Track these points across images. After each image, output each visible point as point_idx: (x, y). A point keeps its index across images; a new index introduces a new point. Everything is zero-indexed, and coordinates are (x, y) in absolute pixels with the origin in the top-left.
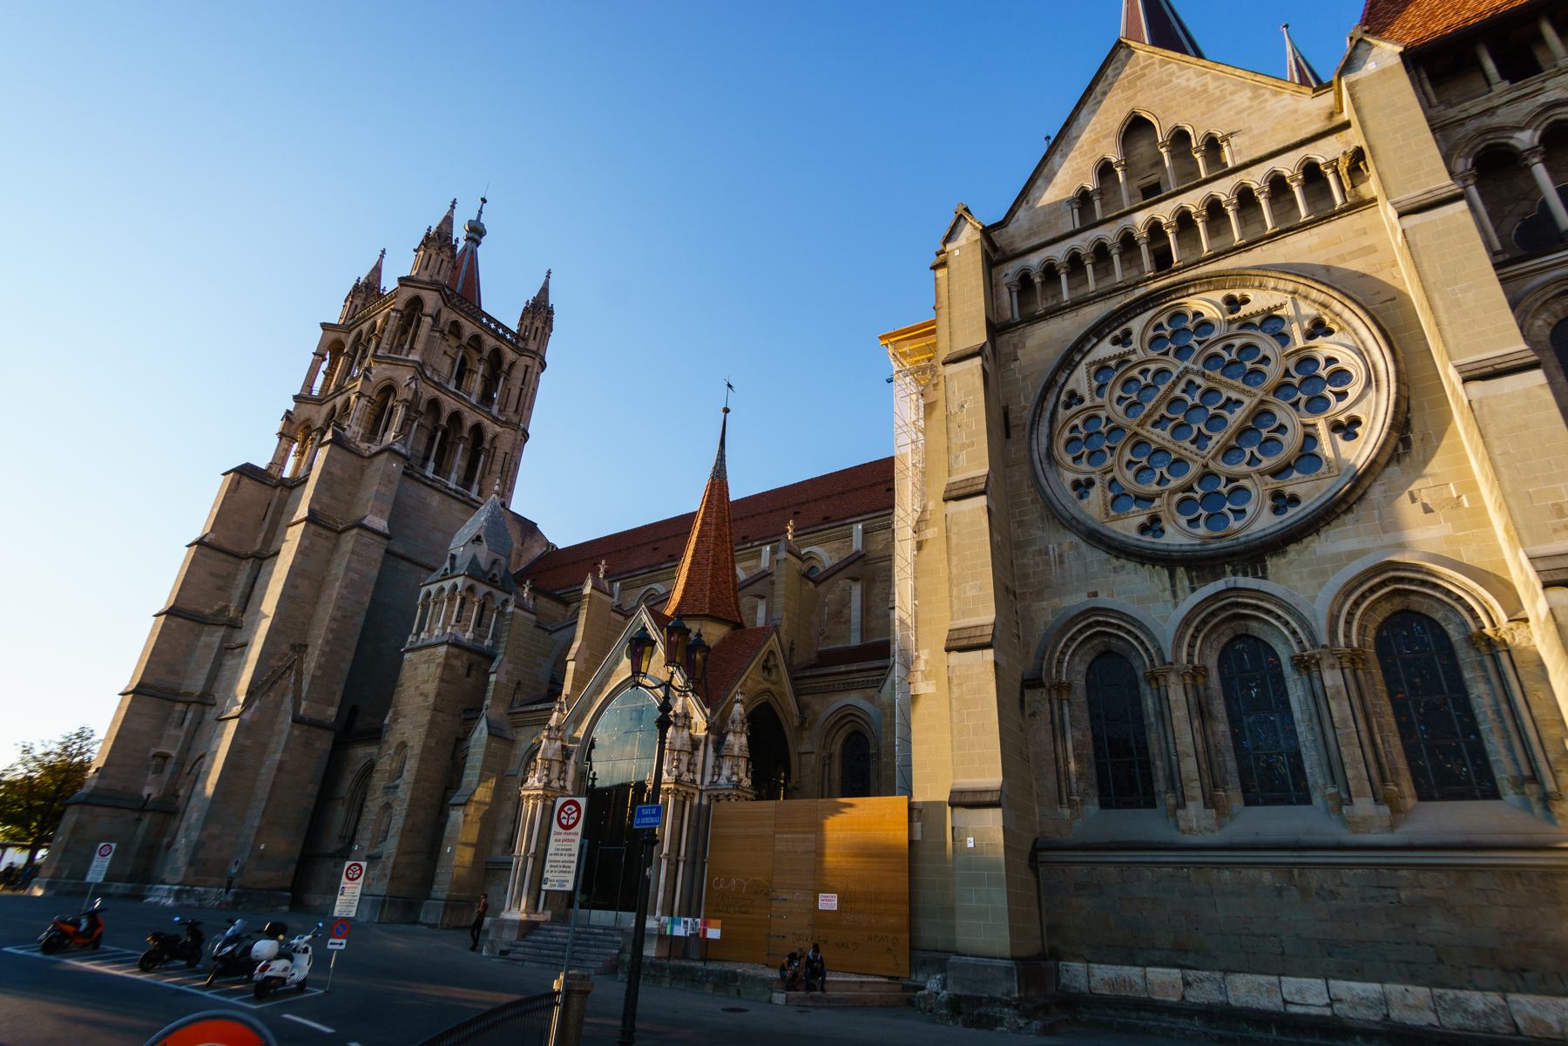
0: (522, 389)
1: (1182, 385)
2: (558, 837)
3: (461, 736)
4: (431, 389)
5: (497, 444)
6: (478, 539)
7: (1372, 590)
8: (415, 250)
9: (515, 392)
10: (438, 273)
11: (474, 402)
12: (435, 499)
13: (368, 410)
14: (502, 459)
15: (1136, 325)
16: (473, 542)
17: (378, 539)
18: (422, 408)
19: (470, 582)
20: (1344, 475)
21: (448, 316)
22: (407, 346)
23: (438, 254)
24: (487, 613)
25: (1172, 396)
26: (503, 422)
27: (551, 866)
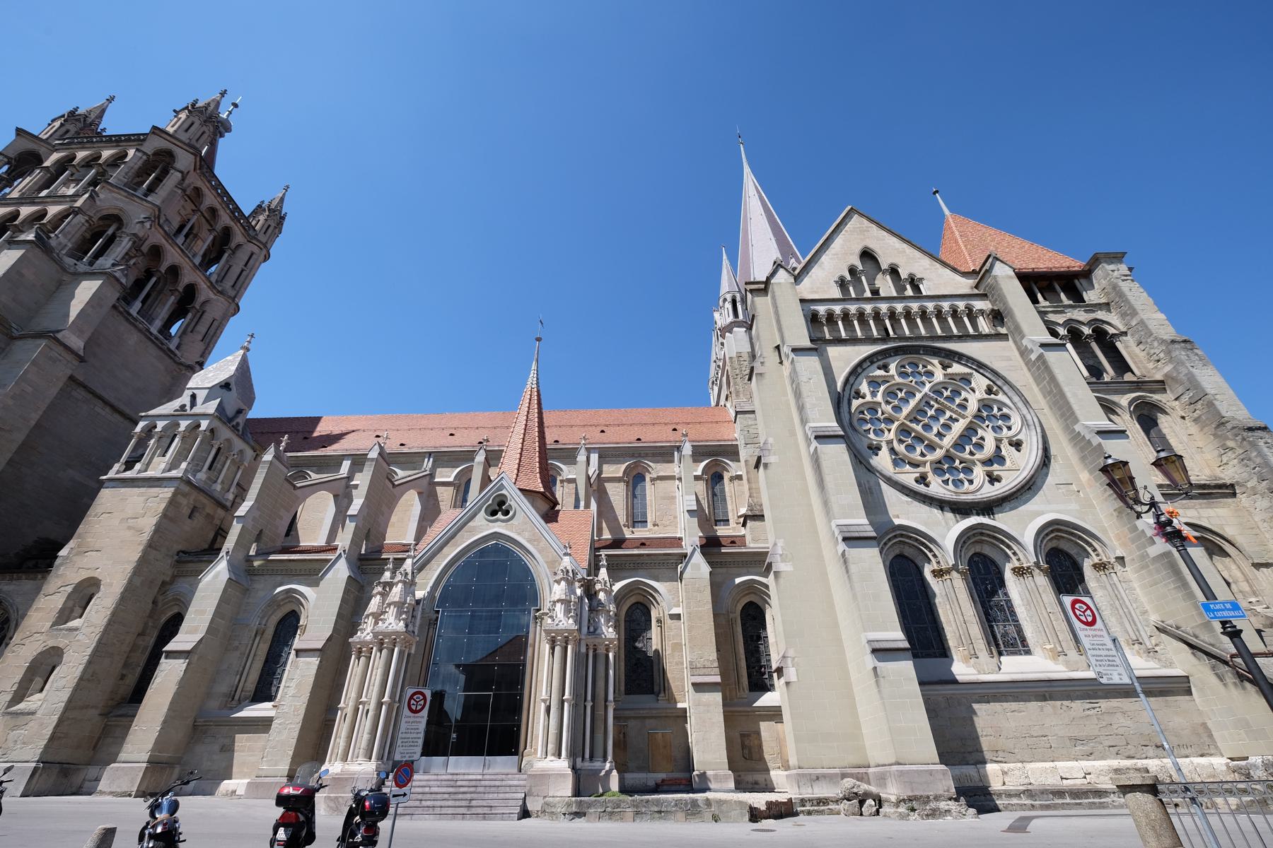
0: (242, 271)
1: (923, 403)
2: (1086, 633)
3: (168, 579)
4: (159, 236)
5: (207, 308)
7: (1047, 535)
8: (175, 111)
9: (235, 270)
10: (197, 140)
11: (197, 264)
12: (133, 338)
13: (84, 228)
14: (209, 324)
16: (221, 387)
17: (69, 357)
18: (145, 248)
19: (217, 424)
20: (1023, 470)
21: (195, 180)
24: (221, 458)
25: (919, 408)
26: (219, 292)
27: (1097, 660)
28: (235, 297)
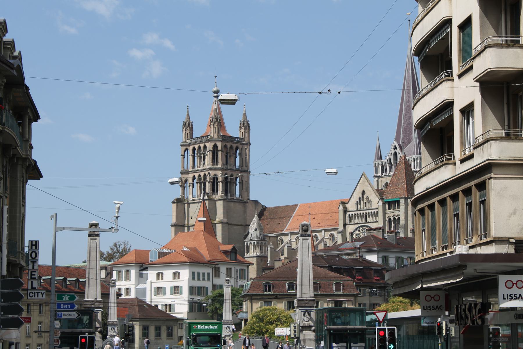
5: (243, 179)
6: (256, 230)
14: (245, 184)
15: (360, 229)
22: (215, 160)
23: (217, 127)
28: (248, 169)
